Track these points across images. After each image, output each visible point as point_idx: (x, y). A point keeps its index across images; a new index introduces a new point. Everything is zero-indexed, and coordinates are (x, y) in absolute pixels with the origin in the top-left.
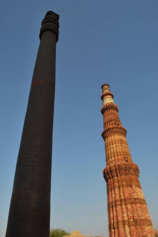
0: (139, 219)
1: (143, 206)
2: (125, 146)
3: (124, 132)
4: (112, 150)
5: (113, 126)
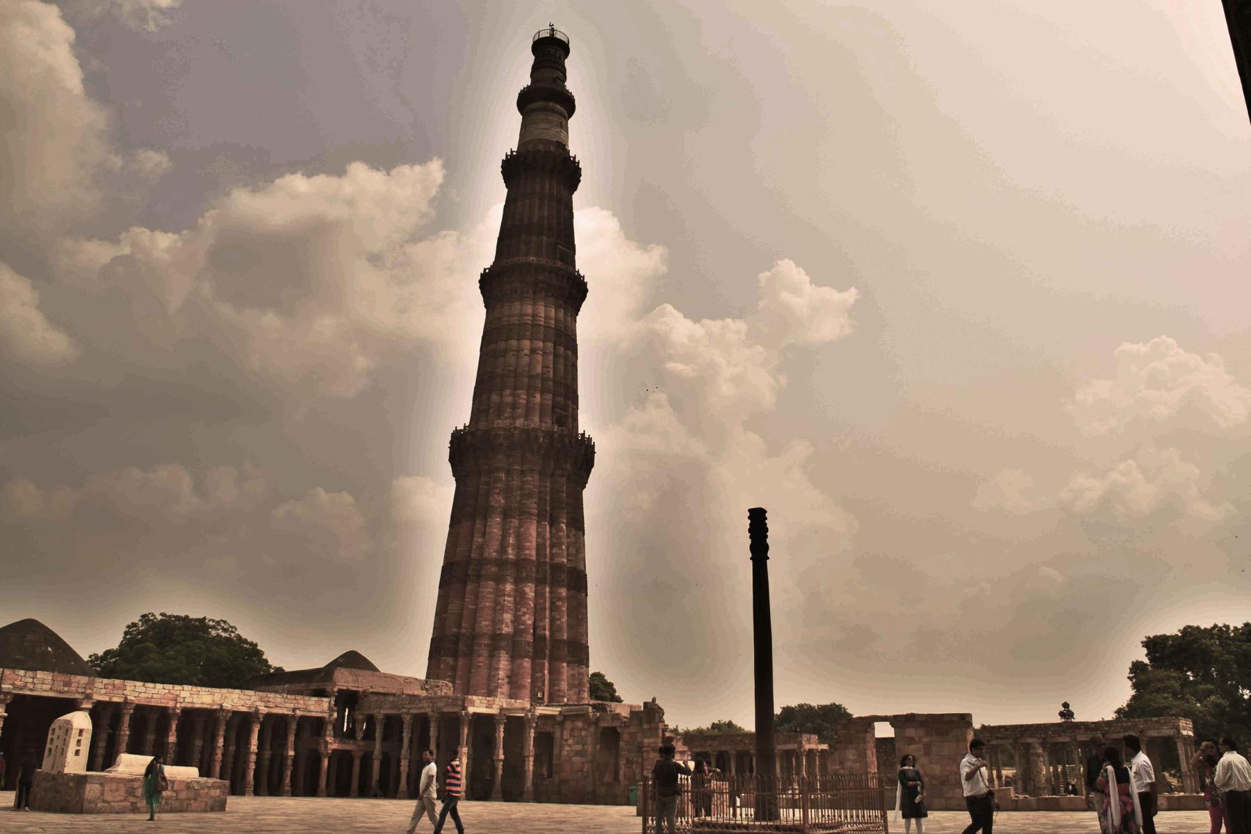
2: (566, 358)
4: (512, 359)
5: (544, 261)
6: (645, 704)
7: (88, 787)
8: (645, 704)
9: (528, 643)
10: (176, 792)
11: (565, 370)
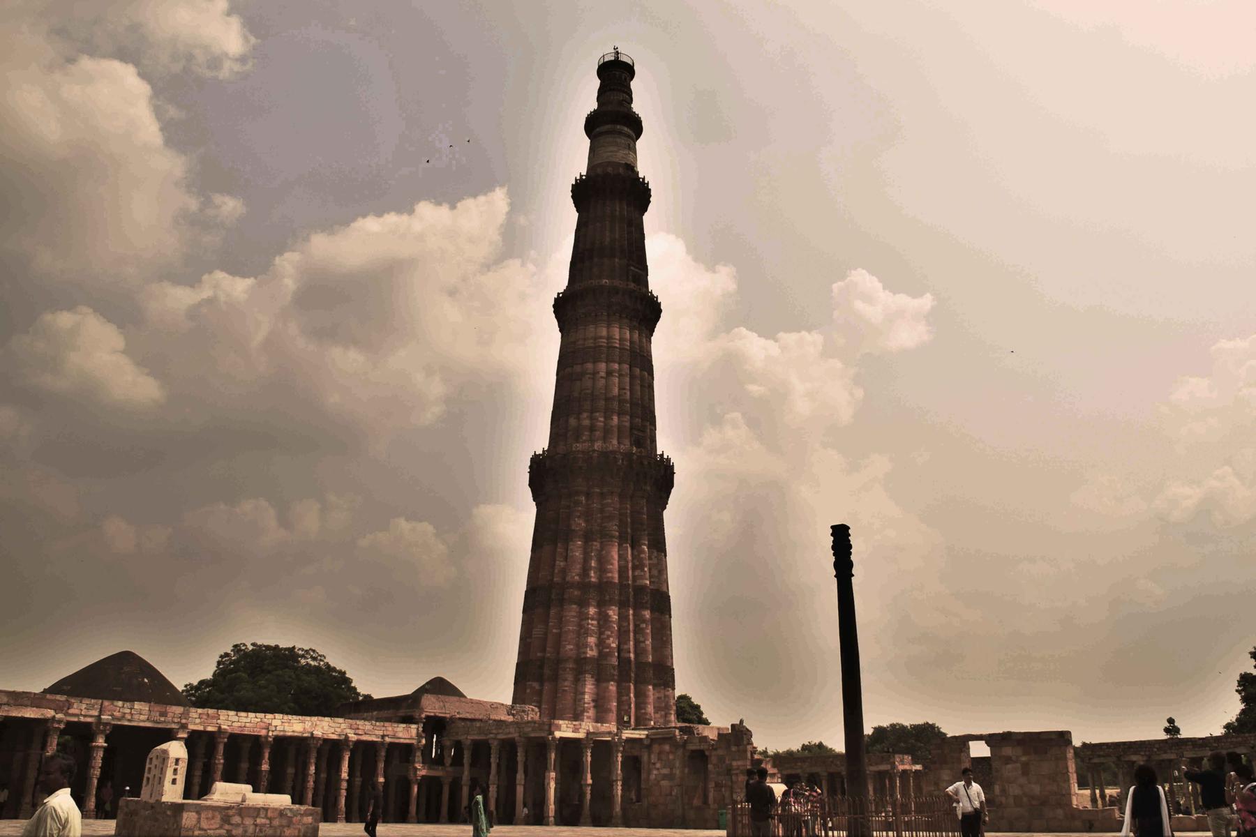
2: (642, 379)
4: (588, 383)
5: (617, 283)
6: (733, 726)
7: (185, 815)
8: (733, 726)
9: (614, 667)
10: (270, 819)
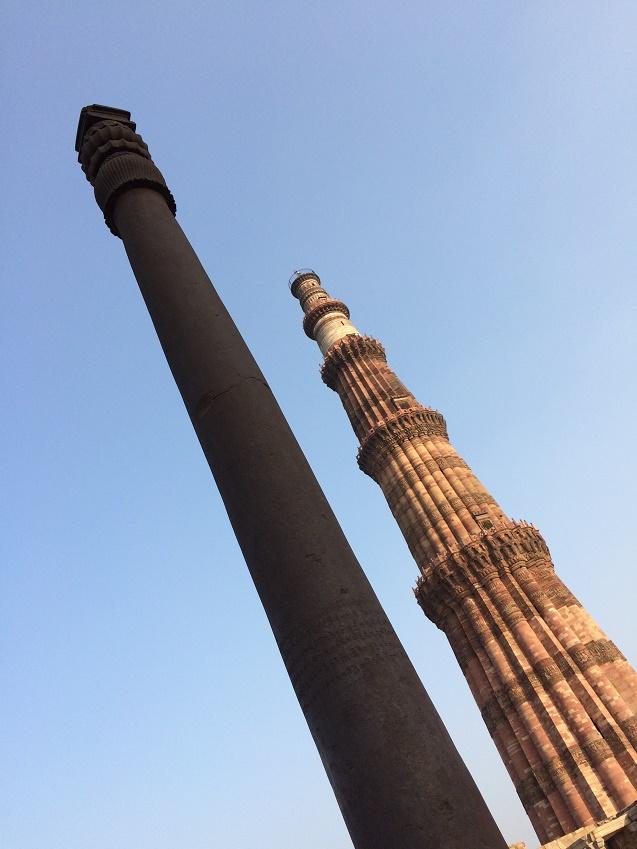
0: (617, 721)
1: (614, 668)
2: (458, 475)
3: (435, 424)
4: (418, 505)
11: (464, 484)
